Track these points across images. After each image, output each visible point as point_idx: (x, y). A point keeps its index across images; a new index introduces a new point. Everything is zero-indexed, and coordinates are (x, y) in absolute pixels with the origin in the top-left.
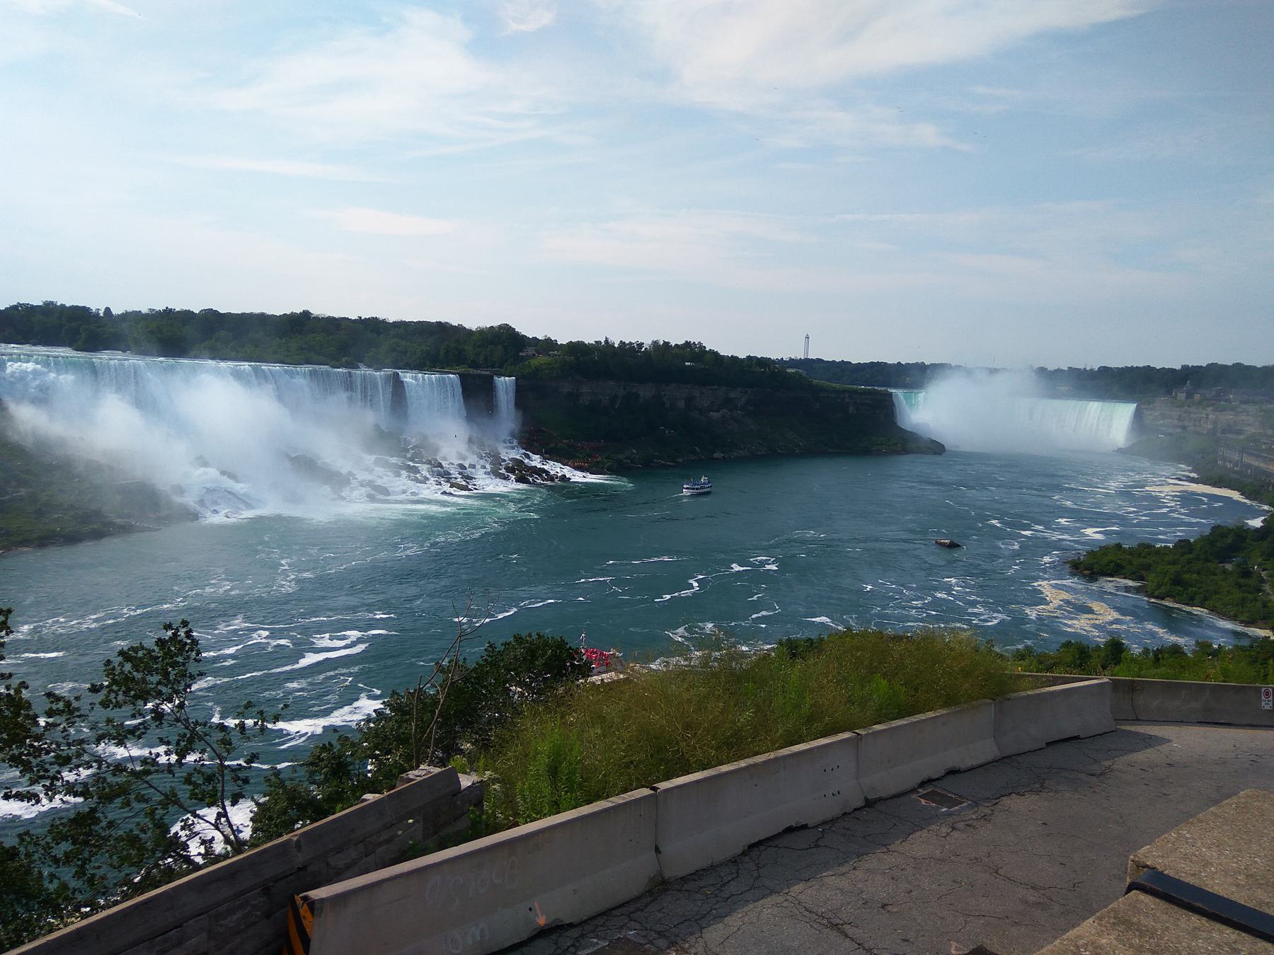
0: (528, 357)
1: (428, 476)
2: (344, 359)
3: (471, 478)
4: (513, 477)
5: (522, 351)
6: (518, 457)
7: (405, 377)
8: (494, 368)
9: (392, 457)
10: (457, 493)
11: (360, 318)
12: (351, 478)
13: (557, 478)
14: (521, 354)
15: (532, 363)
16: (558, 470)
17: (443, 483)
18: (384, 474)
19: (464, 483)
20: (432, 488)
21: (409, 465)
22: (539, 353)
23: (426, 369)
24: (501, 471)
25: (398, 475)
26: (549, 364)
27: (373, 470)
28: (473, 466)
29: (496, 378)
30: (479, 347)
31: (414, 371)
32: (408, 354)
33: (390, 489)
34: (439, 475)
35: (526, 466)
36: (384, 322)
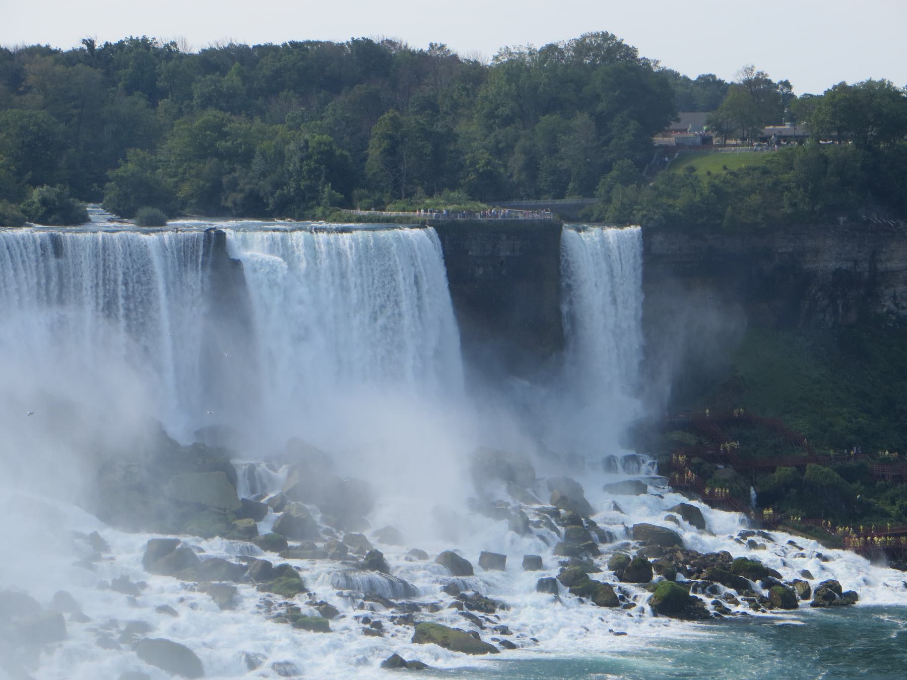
0: (684, 150)
1: (336, 602)
2: (36, 194)
3: (489, 606)
4: (642, 596)
5: (661, 127)
6: (659, 521)
7: (245, 243)
8: (561, 196)
9: (208, 536)
10: (441, 664)
11: (90, 44)
12: (67, 616)
13: (806, 596)
14: (659, 140)
15: (701, 172)
16: (811, 565)
17: (387, 624)
18: (182, 600)
19: (464, 625)
20: (354, 646)
21: (267, 565)
22: (726, 133)
23: (319, 211)
24: (595, 577)
25: (229, 601)
26: (765, 172)
27: (143, 585)
28: (495, 560)
29: (569, 232)
30: (508, 121)
31: (279, 223)
32: (257, 163)
33: (202, 654)
34: (374, 595)
35: (691, 555)
36: (169, 53)
